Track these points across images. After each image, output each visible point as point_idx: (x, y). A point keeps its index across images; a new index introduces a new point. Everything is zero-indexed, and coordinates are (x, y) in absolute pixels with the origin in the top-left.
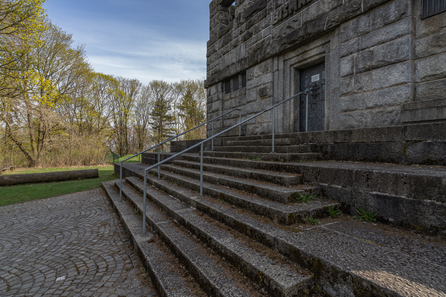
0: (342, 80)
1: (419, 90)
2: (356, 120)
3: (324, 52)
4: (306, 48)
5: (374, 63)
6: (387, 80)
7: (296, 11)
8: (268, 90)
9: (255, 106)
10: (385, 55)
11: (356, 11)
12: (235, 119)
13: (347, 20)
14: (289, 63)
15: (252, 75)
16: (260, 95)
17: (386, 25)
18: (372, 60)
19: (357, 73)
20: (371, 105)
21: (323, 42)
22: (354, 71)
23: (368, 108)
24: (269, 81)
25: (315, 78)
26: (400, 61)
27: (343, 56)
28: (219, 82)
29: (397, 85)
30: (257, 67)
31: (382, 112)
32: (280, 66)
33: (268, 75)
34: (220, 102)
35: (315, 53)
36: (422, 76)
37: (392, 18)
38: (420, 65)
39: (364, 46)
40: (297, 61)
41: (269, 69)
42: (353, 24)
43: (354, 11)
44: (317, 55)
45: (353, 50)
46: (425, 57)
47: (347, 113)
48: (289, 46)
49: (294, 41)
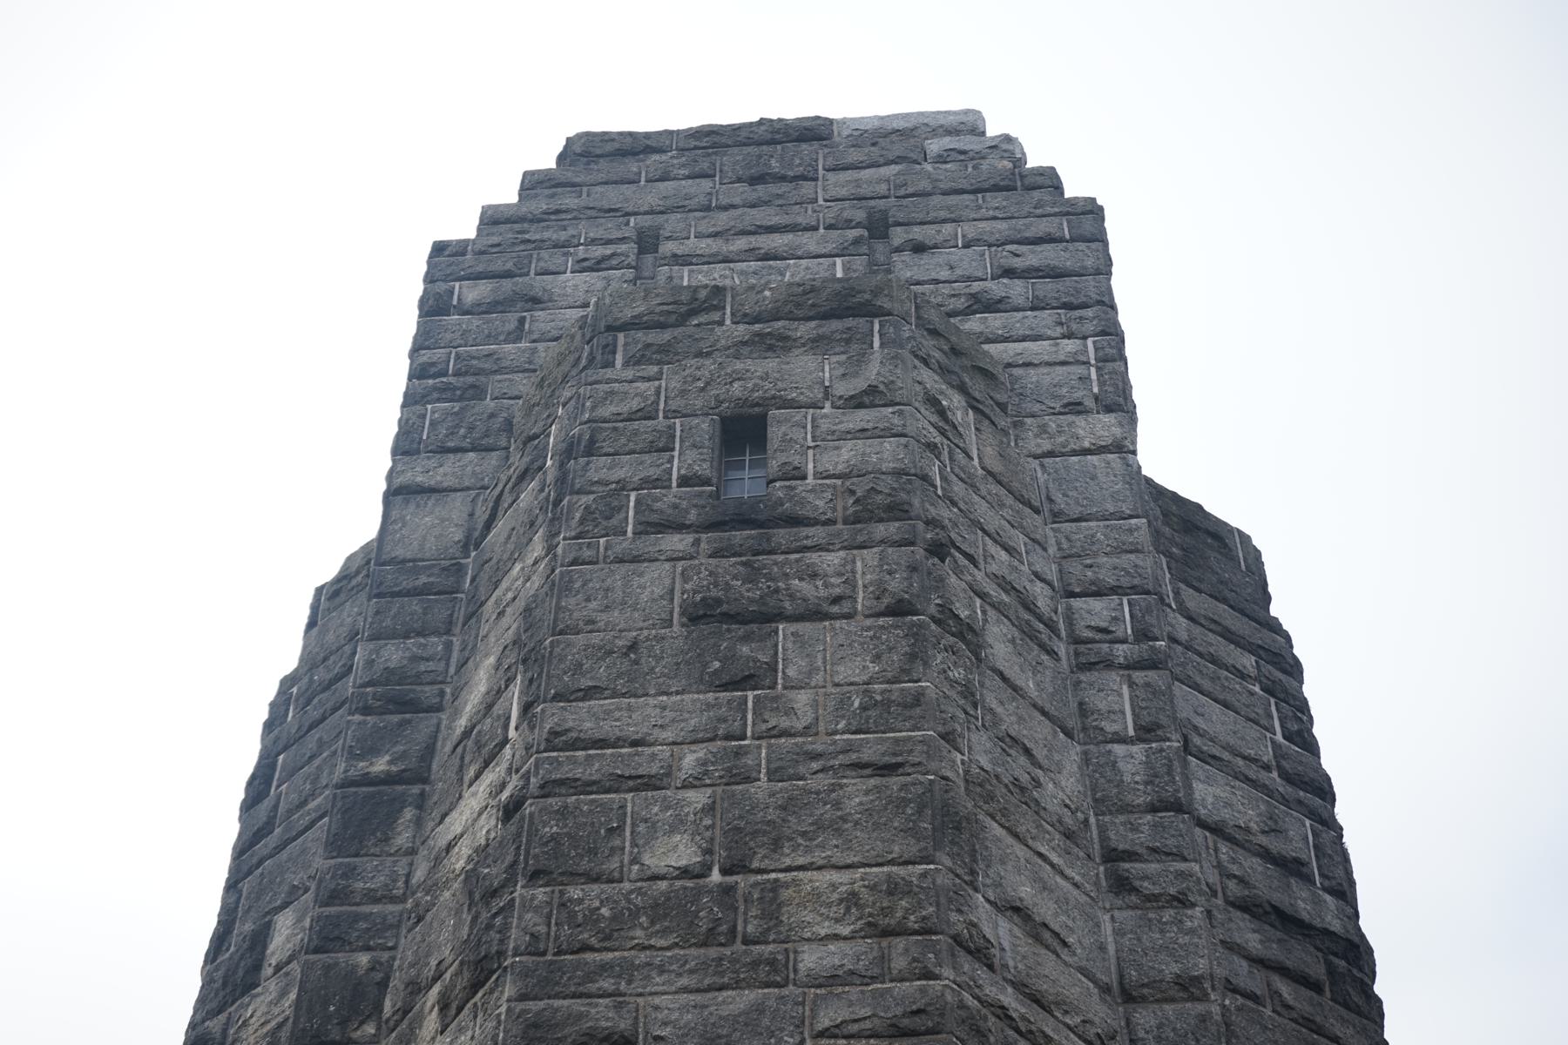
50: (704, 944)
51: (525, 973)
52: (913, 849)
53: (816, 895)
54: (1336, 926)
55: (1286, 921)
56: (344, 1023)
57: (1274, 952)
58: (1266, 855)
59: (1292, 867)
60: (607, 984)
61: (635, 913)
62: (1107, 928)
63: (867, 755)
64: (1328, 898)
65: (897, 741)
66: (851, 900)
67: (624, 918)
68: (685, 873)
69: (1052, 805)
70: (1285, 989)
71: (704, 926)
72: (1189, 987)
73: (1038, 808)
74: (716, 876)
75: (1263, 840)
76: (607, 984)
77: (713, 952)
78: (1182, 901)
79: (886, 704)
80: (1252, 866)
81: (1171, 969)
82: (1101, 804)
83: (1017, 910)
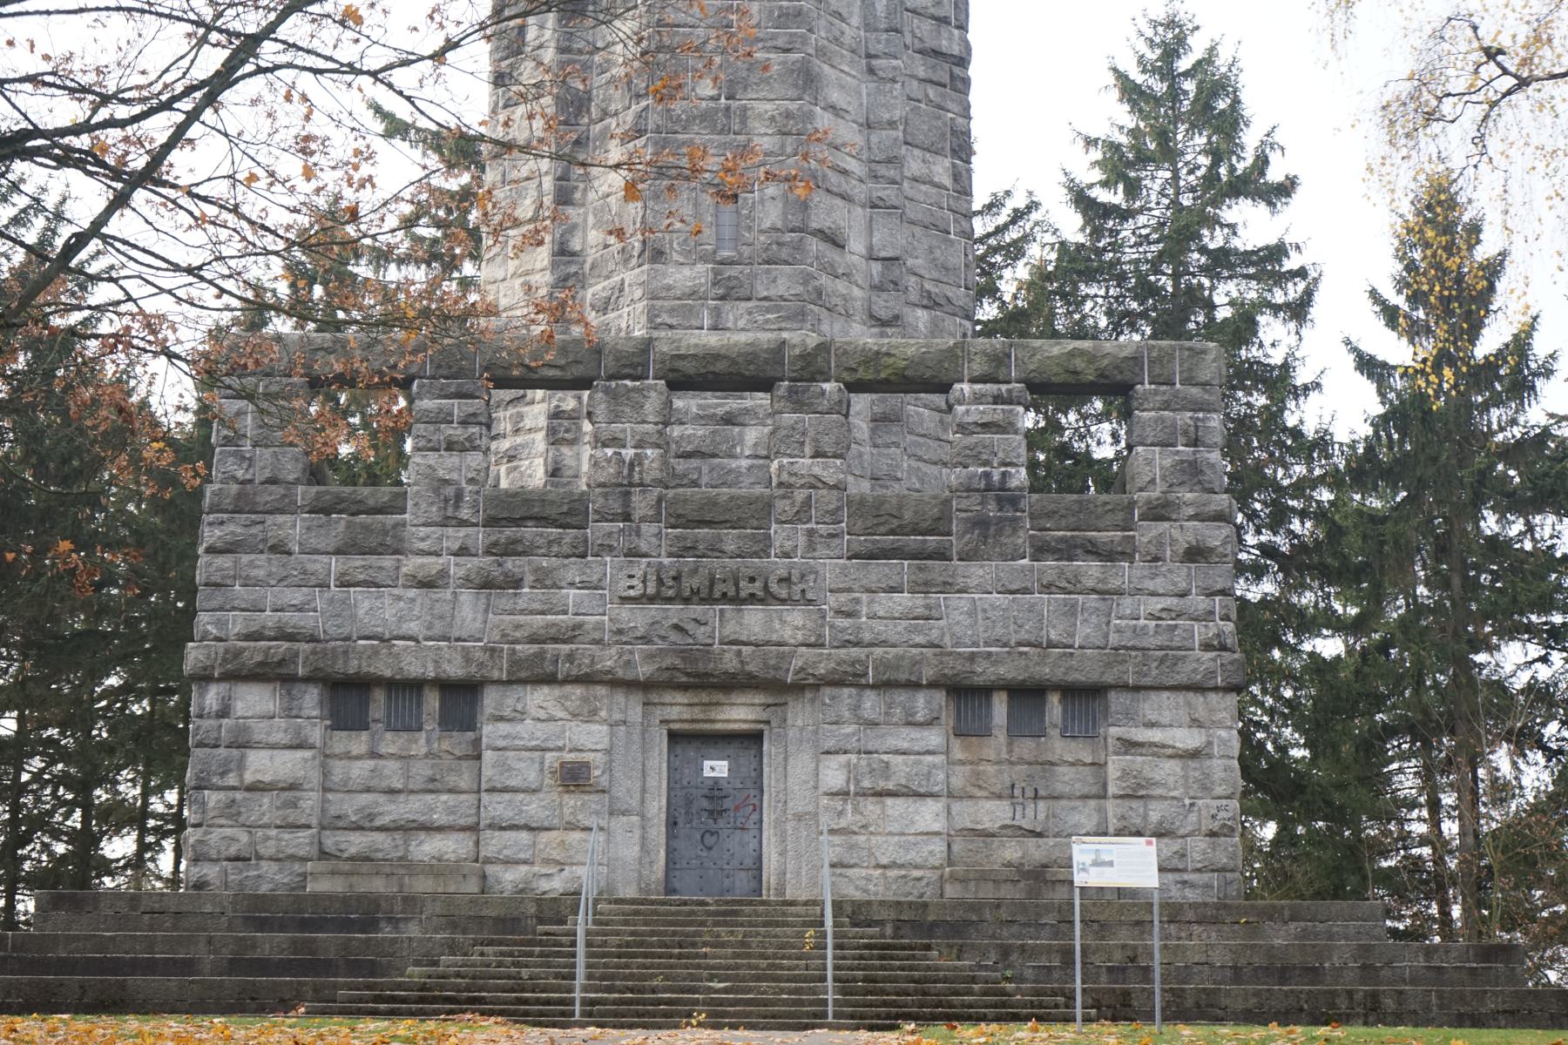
0: (825, 801)
1: (955, 848)
2: (857, 888)
3: (768, 722)
4: (721, 697)
5: (890, 786)
6: (913, 822)
7: (703, 601)
8: (597, 773)
9: (534, 808)
10: (909, 776)
11: (860, 676)
12: (398, 835)
13: (838, 683)
14: (659, 713)
15: (519, 708)
16: (563, 779)
17: (909, 724)
18: (887, 778)
19: (857, 794)
20: (884, 861)
21: (770, 701)
22: (852, 788)
23: (878, 866)
24: (598, 747)
25: (717, 768)
26: (932, 795)
27: (828, 753)
28: (307, 680)
29: (927, 834)
30: (546, 689)
31: (904, 877)
32: (630, 712)
33: (594, 727)
34: (314, 758)
35: (742, 716)
36: (959, 827)
37: (919, 717)
38: (957, 807)
39: (870, 748)
40: (685, 716)
41: (603, 714)
42: (850, 696)
43: (855, 675)
44: (745, 721)
45: (849, 747)
46: (961, 798)
47: (839, 871)
48: (684, 679)
49: (706, 674)
50: (721, 132)
51: (656, 143)
52: (795, 95)
53: (760, 115)
54: (956, 50)
55: (937, 53)
56: (576, 116)
57: (930, 75)
58: (933, 17)
59: (944, 21)
60: (684, 150)
61: (695, 118)
62: (864, 92)
63: (780, 42)
64: (956, 32)
65: (791, 35)
66: (772, 118)
67: (691, 120)
68: (712, 98)
69: (847, 40)
70: (932, 92)
71: (719, 127)
72: (892, 124)
73: (841, 45)
74: (723, 100)
75: (932, 10)
76: (684, 150)
77: (723, 138)
78: (894, 81)
79: (787, 15)
80: (925, 27)
81: (886, 116)
82: (868, 27)
83: (833, 108)
